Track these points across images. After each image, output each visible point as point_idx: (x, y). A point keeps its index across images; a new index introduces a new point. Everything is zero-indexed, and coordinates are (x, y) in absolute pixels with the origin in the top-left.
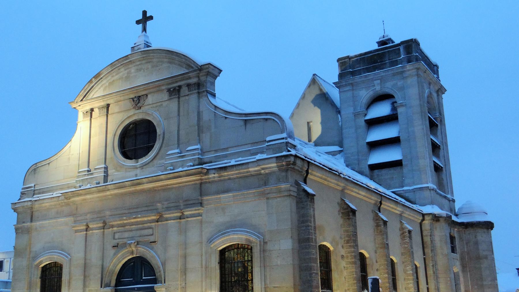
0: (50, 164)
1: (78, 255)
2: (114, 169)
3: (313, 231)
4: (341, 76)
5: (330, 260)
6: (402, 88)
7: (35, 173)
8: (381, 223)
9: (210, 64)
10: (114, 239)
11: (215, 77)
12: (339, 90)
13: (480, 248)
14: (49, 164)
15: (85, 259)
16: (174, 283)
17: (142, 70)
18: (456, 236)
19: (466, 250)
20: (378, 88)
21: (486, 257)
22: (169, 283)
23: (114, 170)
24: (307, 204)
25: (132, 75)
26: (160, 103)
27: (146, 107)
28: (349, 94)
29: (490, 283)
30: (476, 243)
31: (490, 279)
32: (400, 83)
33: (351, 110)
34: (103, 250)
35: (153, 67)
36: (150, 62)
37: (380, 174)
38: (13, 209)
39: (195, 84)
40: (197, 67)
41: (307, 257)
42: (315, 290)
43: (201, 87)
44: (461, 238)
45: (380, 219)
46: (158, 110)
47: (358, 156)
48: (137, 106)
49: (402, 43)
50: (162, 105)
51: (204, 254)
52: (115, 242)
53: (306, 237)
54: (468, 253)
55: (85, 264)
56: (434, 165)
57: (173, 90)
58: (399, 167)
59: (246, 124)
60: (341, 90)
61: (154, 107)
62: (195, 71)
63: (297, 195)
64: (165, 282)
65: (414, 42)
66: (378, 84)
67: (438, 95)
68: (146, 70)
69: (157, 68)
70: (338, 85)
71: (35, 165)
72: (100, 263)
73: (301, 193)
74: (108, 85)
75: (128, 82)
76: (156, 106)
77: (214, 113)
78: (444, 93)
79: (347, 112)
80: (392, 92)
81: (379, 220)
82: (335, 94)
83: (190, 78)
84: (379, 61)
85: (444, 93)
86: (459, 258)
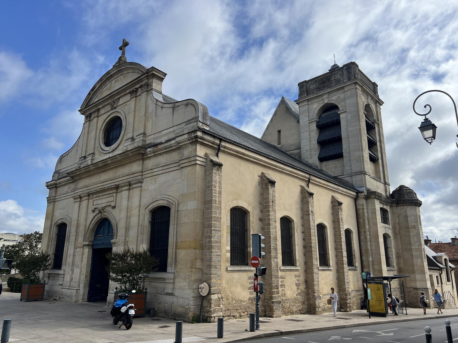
1: (75, 217)
3: (217, 195)
4: (300, 95)
5: (248, 221)
6: (344, 100)
8: (307, 195)
9: (153, 67)
10: (93, 205)
11: (162, 79)
12: (299, 106)
13: (409, 219)
15: (78, 220)
18: (389, 211)
19: (397, 222)
20: (326, 101)
21: (414, 227)
24: (212, 172)
25: (113, 85)
27: (119, 107)
28: (306, 108)
29: (417, 247)
30: (406, 217)
31: (417, 244)
32: (342, 96)
33: (307, 119)
35: (124, 77)
36: (122, 75)
37: (327, 164)
38: (46, 186)
39: (145, 85)
41: (209, 216)
42: (214, 244)
43: (149, 87)
44: (393, 213)
45: (306, 192)
47: (311, 152)
49: (344, 66)
50: (127, 104)
51: (141, 215)
53: (210, 199)
54: (399, 224)
55: (77, 224)
56: (370, 156)
58: (341, 159)
59: (173, 111)
60: (300, 105)
61: (122, 107)
63: (206, 165)
65: (353, 64)
66: (326, 98)
67: (376, 106)
70: (298, 102)
72: (85, 223)
73: (209, 163)
76: (124, 106)
78: (382, 105)
79: (304, 120)
80: (336, 103)
81: (306, 193)
82: (295, 108)
84: (327, 81)
85: (381, 105)
86: (391, 228)
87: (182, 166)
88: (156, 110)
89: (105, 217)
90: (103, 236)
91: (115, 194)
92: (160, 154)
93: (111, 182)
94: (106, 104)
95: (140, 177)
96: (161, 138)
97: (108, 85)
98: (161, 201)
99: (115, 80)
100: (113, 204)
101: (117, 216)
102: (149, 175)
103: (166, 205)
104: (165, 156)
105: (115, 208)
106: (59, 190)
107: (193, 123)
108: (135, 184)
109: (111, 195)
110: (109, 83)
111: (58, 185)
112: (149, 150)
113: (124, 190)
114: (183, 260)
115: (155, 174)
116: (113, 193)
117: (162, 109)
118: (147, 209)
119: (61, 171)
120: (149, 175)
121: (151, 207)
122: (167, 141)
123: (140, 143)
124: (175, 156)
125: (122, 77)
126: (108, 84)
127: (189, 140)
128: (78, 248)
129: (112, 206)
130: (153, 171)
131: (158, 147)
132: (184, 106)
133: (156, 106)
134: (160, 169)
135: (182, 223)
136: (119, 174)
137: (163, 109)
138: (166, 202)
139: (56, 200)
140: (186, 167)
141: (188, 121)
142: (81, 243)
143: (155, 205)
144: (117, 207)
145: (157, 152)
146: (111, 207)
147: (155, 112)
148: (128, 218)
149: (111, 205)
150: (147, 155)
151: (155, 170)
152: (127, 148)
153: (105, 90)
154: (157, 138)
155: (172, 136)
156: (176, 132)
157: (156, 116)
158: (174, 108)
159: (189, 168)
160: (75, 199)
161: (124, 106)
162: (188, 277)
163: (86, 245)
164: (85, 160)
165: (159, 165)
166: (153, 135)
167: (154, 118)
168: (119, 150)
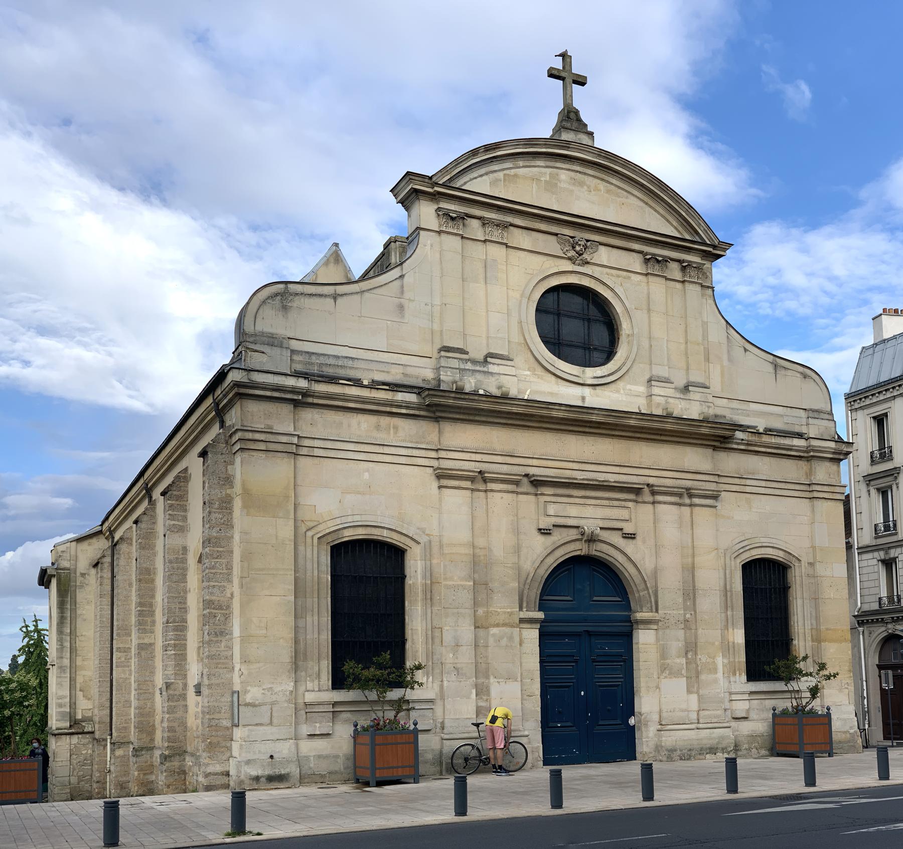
0: (339, 300)
2: (529, 370)
7: (285, 308)
14: (335, 299)
16: (674, 612)
17: (585, 187)
22: (666, 612)
23: (528, 373)
26: (625, 273)
34: (517, 531)
35: (608, 191)
40: (710, 239)
46: (621, 284)
48: (580, 258)
52: (545, 523)
57: (650, 259)
59: (776, 371)
62: (705, 244)
64: (657, 611)
68: (594, 190)
69: (619, 199)
71: (282, 286)
74: (502, 178)
75: (554, 196)
77: (726, 334)
83: (688, 250)
87: (816, 495)
88: (728, 345)
89: (594, 553)
90: (572, 601)
91: (630, 504)
92: (757, 453)
93: (617, 469)
94: (543, 226)
95: (713, 486)
96: (748, 416)
97: (541, 170)
98: (771, 549)
99: (572, 174)
100: (628, 528)
101: (644, 558)
102: (734, 488)
103: (781, 560)
104: (767, 459)
105: (634, 538)
106: (308, 415)
107: (827, 421)
108: (699, 498)
109: (616, 503)
110: (547, 167)
111: (310, 400)
112: (739, 435)
113: (665, 503)
114: (833, 660)
115: (748, 489)
116: (625, 500)
117: (745, 352)
118: (738, 561)
119: (295, 345)
120: (734, 488)
121: (747, 557)
122: (768, 431)
123: (709, 407)
124: (791, 470)
125: (602, 185)
126: (539, 166)
127: (834, 453)
128: (498, 625)
129: (625, 531)
130: (743, 482)
131: (761, 437)
132: (798, 375)
133: (728, 337)
134: (763, 484)
135: (826, 597)
136: (641, 457)
137: (748, 353)
138: (781, 554)
139: (304, 451)
140: (824, 500)
141: (813, 411)
142: (511, 614)
143: (757, 554)
144: (638, 538)
145: (755, 445)
146: (620, 533)
147: (728, 351)
148: (690, 570)
149: (621, 529)
150: (729, 443)
151: (748, 482)
152: (667, 402)
153: (525, 177)
154: (740, 411)
155: (778, 424)
156: (786, 419)
157: (730, 360)
158: (776, 366)
159: (830, 503)
160: (439, 477)
161: (618, 276)
162: (846, 686)
163: (531, 621)
164: (485, 369)
165: (753, 474)
166: (726, 400)
167: (726, 363)
168: (618, 391)
